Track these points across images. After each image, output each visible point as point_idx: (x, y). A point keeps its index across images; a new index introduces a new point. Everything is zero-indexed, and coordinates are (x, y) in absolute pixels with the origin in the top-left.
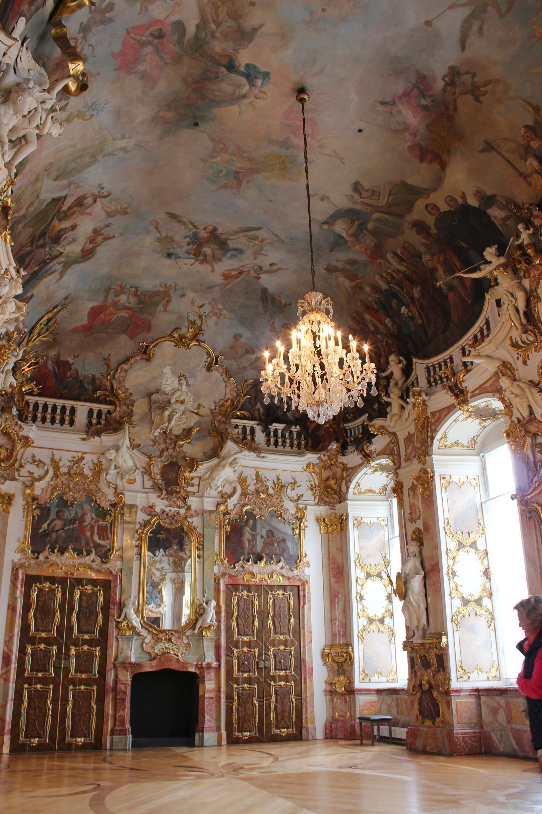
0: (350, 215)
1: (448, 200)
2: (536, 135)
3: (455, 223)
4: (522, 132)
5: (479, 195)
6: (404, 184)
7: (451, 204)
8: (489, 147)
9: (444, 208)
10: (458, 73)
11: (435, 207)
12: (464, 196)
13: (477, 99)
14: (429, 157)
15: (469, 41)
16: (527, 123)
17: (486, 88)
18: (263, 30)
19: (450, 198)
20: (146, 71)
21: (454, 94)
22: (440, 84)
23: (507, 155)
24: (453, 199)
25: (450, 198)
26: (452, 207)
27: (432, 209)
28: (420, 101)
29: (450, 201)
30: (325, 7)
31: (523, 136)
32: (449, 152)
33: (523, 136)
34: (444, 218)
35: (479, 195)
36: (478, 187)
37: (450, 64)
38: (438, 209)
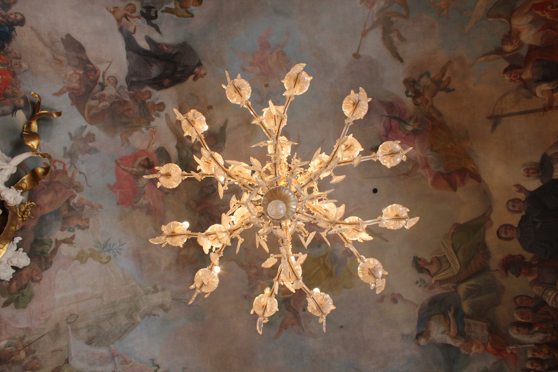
0: (434, 309)
1: (510, 207)
2: (519, 67)
3: (538, 226)
4: (507, 78)
5: (531, 171)
6: (459, 228)
7: (516, 209)
8: (495, 119)
9: (515, 220)
10: (414, 82)
11: (507, 227)
12: (520, 188)
13: (449, 91)
14: (458, 179)
15: (400, 51)
16: (503, 69)
17: (447, 75)
18: (229, 126)
19: (510, 203)
20: (149, 204)
21: (427, 101)
22: (408, 102)
23: (514, 110)
24: (514, 201)
25: (510, 203)
26: (520, 212)
27: (506, 233)
28: (405, 129)
29: (514, 206)
30: (266, 83)
31: (511, 81)
32: (469, 158)
33: (511, 81)
34: (524, 231)
35: (531, 171)
36: (524, 165)
37: (402, 79)
38: (511, 227)
